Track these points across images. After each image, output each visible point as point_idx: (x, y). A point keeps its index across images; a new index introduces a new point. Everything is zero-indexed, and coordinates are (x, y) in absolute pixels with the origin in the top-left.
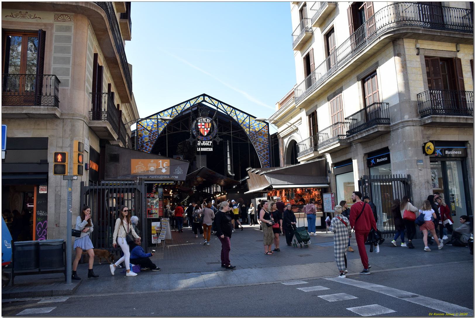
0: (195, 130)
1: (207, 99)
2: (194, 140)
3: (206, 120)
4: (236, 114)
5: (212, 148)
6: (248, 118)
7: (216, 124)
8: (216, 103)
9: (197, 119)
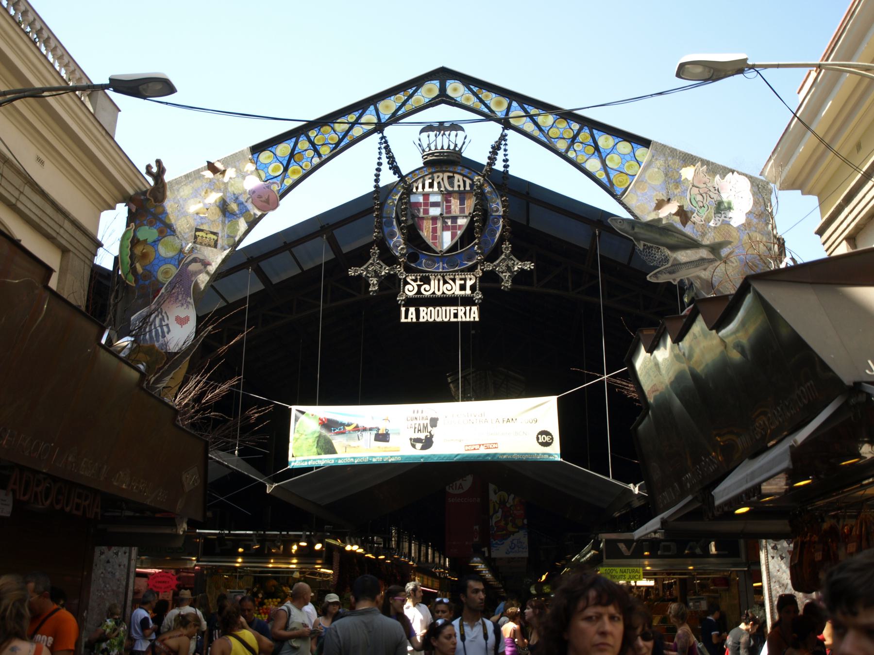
4: (597, 148)
5: (475, 309)
8: (499, 104)
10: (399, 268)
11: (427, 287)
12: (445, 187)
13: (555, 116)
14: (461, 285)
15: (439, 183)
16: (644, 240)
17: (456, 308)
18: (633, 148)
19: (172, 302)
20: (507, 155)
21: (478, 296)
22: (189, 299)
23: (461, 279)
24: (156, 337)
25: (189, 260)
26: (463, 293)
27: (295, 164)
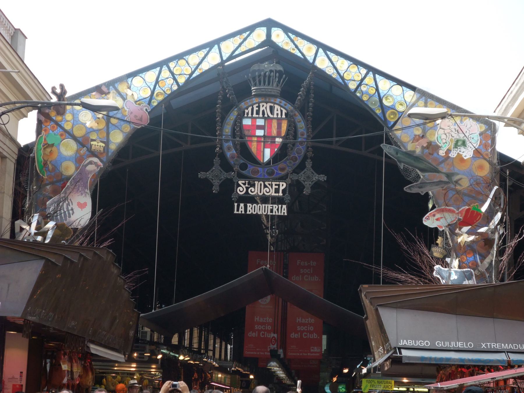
0: (231, 144)
2: (225, 175)
3: (272, 109)
4: (377, 90)
5: (284, 207)
7: (307, 125)
8: (310, 49)
9: (243, 105)
11: (253, 189)
13: (349, 62)
14: (275, 189)
15: (263, 111)
16: (404, 162)
17: (272, 205)
18: (403, 90)
19: (75, 192)
21: (288, 198)
22: (86, 190)
23: (276, 185)
24: (64, 217)
25: (87, 162)
26: (277, 194)
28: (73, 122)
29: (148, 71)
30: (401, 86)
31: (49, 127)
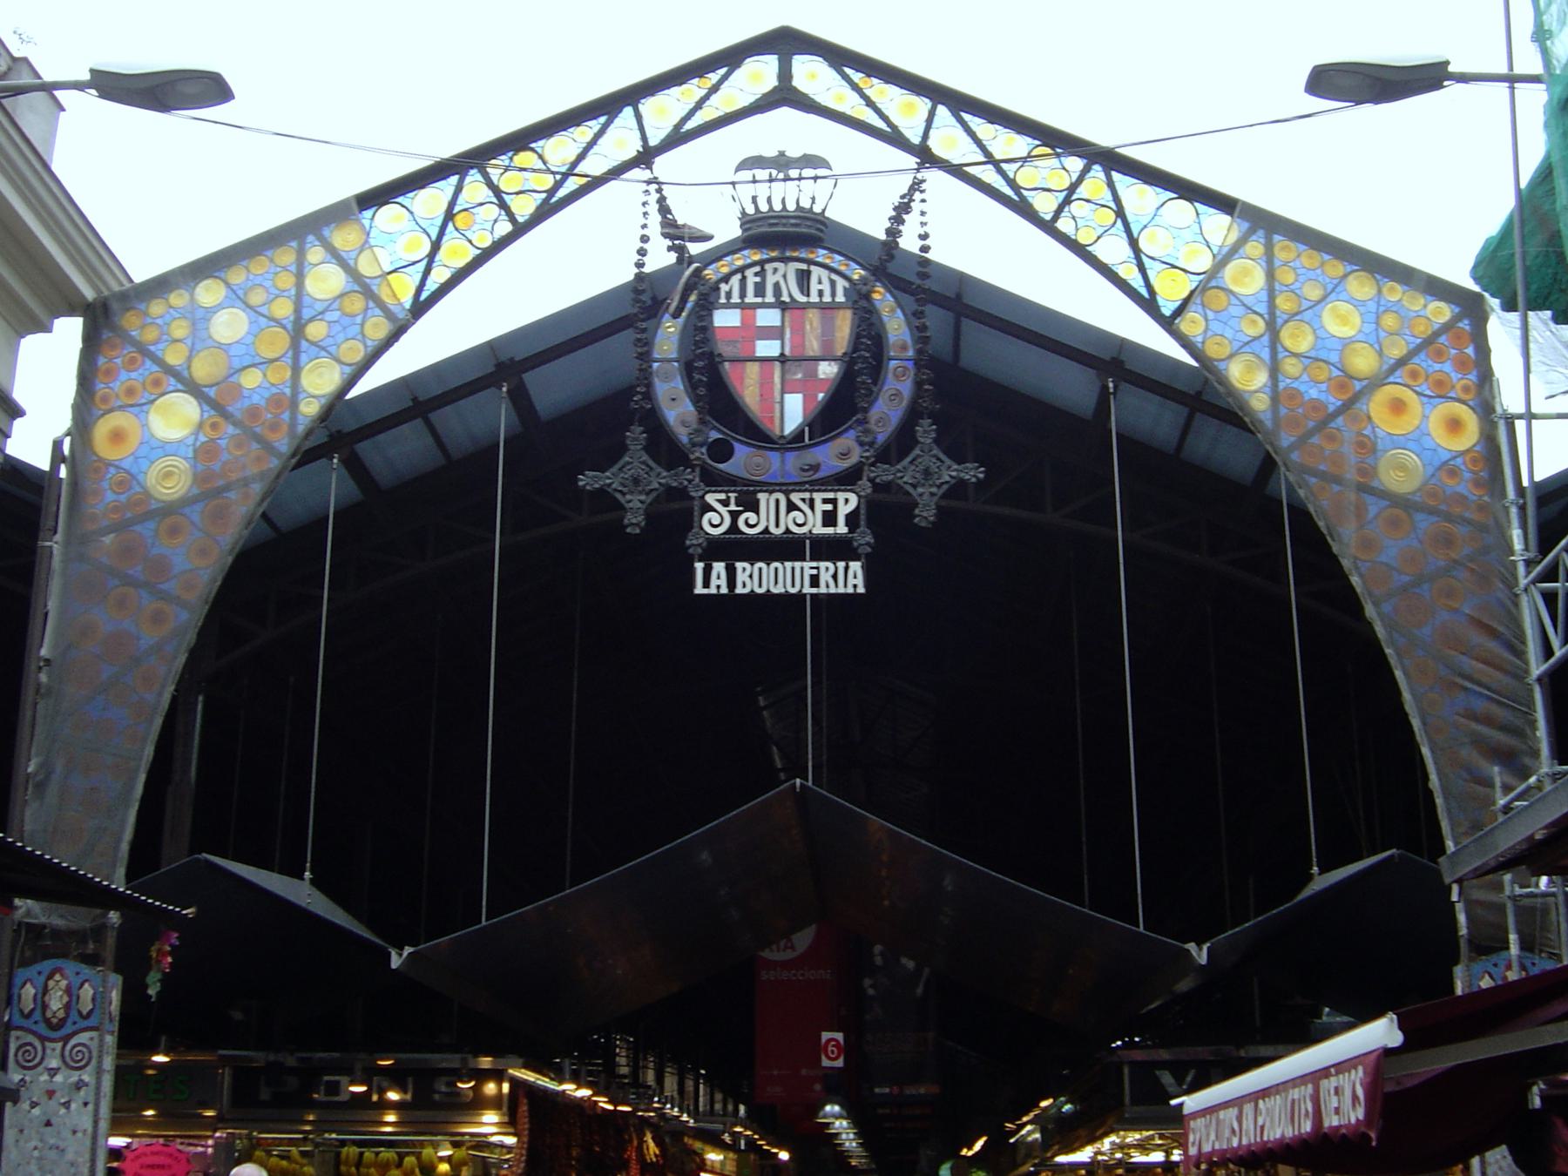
1: (811, 74)
2: (660, 478)
3: (804, 278)
4: (1120, 213)
5: (856, 566)
6: (1255, 247)
10: (689, 474)
12: (790, 296)
13: (1029, 140)
14: (825, 512)
15: (777, 286)
17: (814, 564)
18: (1198, 214)
20: (926, 224)
21: (865, 538)
23: (825, 501)
26: (830, 530)
27: (456, 234)
28: (193, 344)
29: (423, 187)
30: (1190, 200)
31: (118, 361)
